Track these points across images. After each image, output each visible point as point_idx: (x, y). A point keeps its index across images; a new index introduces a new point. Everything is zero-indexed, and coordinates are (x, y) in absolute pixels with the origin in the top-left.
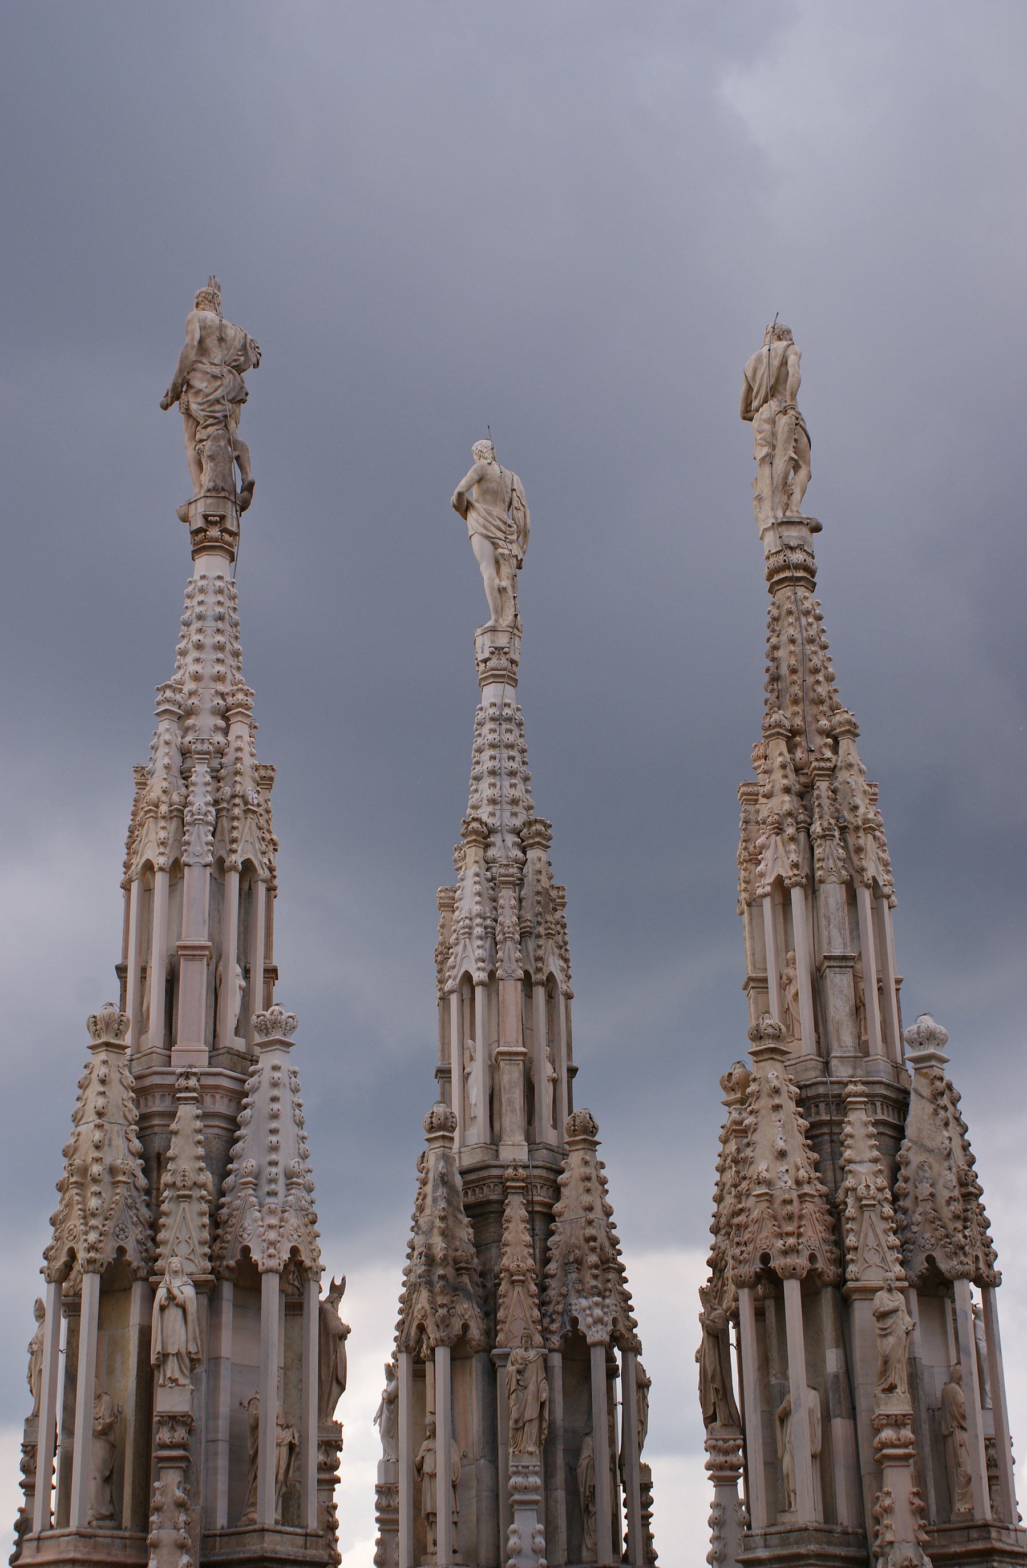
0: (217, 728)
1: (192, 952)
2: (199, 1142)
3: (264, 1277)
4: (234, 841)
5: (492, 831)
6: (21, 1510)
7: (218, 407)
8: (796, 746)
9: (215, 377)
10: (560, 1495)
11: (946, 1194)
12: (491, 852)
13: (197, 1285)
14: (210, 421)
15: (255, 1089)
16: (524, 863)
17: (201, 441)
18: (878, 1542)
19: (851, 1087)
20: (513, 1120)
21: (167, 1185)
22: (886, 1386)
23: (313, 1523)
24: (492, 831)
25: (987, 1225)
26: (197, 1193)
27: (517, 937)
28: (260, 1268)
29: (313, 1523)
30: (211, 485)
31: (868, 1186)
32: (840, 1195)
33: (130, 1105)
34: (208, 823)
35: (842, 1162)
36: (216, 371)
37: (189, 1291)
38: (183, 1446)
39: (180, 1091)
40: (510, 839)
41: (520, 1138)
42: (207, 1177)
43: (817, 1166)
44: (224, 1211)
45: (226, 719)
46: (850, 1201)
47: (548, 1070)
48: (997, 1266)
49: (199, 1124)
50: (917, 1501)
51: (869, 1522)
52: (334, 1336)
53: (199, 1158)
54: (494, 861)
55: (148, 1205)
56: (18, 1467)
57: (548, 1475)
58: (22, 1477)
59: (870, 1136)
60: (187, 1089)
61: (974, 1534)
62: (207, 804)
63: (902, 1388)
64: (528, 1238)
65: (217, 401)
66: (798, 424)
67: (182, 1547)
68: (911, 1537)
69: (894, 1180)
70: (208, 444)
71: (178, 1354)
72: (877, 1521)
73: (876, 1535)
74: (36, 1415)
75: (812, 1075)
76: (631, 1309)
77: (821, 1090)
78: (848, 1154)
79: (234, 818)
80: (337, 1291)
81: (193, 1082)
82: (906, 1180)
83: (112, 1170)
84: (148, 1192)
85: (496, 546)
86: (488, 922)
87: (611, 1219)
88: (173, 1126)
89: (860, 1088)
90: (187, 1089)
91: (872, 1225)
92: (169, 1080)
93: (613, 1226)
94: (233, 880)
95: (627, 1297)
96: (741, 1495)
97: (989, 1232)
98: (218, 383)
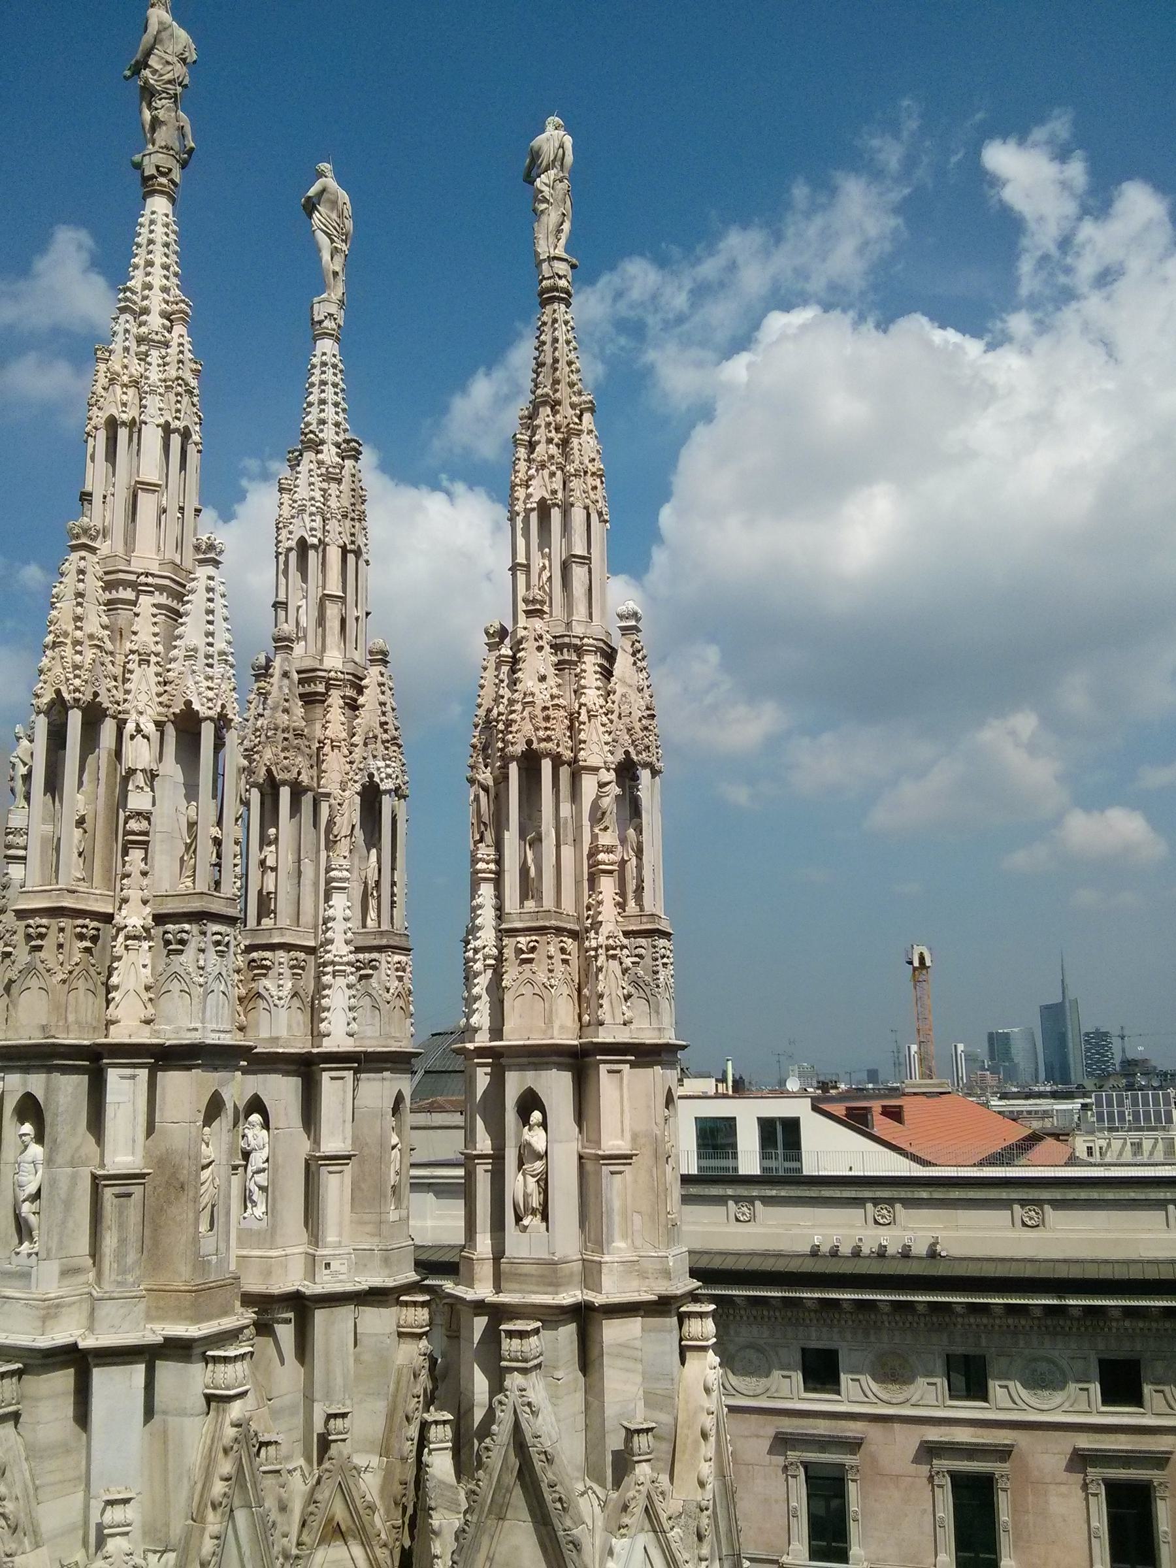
0: (164, 326)
1: (150, 487)
4: (178, 411)
5: (322, 442)
7: (169, 86)
8: (557, 412)
9: (168, 63)
12: (320, 456)
14: (164, 95)
15: (192, 592)
17: (156, 109)
24: (322, 442)
26: (153, 659)
27: (339, 517)
30: (163, 144)
33: (100, 591)
34: (160, 394)
36: (170, 59)
40: (334, 450)
45: (171, 321)
49: (155, 611)
54: (323, 463)
55: (113, 663)
62: (160, 380)
65: (169, 82)
70: (162, 112)
75: (560, 631)
77: (566, 640)
79: (177, 394)
81: (150, 580)
83: (91, 637)
85: (332, 241)
86: (318, 504)
92: (133, 577)
94: (176, 440)
98: (170, 68)
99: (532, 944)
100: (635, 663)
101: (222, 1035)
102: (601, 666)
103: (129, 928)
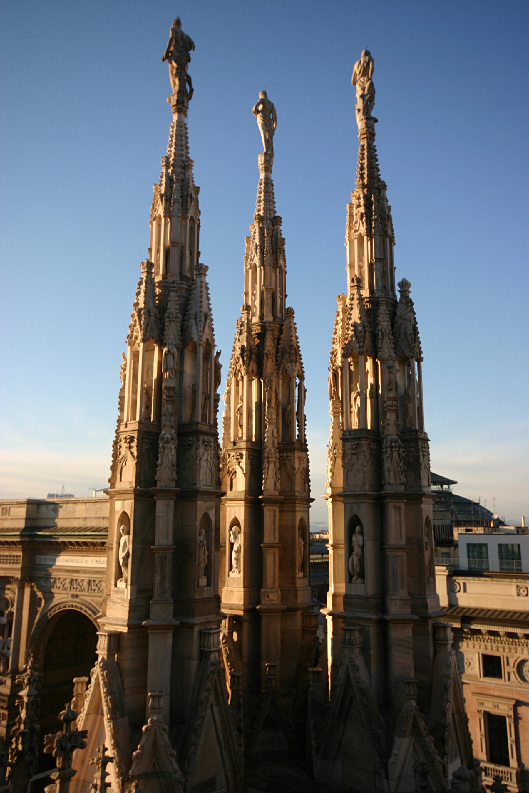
2: (177, 304)
3: (198, 347)
6: (119, 416)
10: (280, 421)
11: (409, 332)
13: (178, 349)
15: (195, 288)
16: (273, 230)
18: (384, 434)
19: (381, 299)
20: (267, 309)
21: (167, 317)
22: (389, 388)
23: (212, 422)
25: (420, 343)
28: (197, 344)
29: (212, 422)
31: (385, 329)
32: (377, 332)
35: (377, 322)
37: (175, 350)
38: (172, 397)
39: (171, 287)
41: (270, 315)
42: (180, 316)
43: (369, 323)
44: (185, 326)
46: (380, 333)
47: (279, 295)
48: (422, 356)
49: (177, 298)
50: (397, 423)
51: (381, 429)
52: (218, 367)
53: (177, 309)
56: (118, 404)
57: (277, 415)
58: (119, 406)
59: (386, 314)
60: (173, 287)
61: (413, 433)
63: (394, 390)
64: (273, 345)
66: (372, 84)
67: (172, 427)
68: (395, 433)
69: (392, 328)
71: (172, 369)
72: (384, 428)
73: (383, 433)
74: (124, 387)
76: (303, 367)
78: (380, 319)
80: (218, 354)
81: (175, 285)
82: (396, 328)
84: (160, 319)
87: (298, 340)
88: (169, 299)
89: (384, 299)
90: (173, 287)
91: (386, 341)
92: (167, 284)
93: (298, 342)
95: (302, 364)
96: (341, 421)
97: (420, 345)
99: (354, 446)
100: (407, 308)
101: (208, 487)
102: (390, 311)
103: (165, 439)
